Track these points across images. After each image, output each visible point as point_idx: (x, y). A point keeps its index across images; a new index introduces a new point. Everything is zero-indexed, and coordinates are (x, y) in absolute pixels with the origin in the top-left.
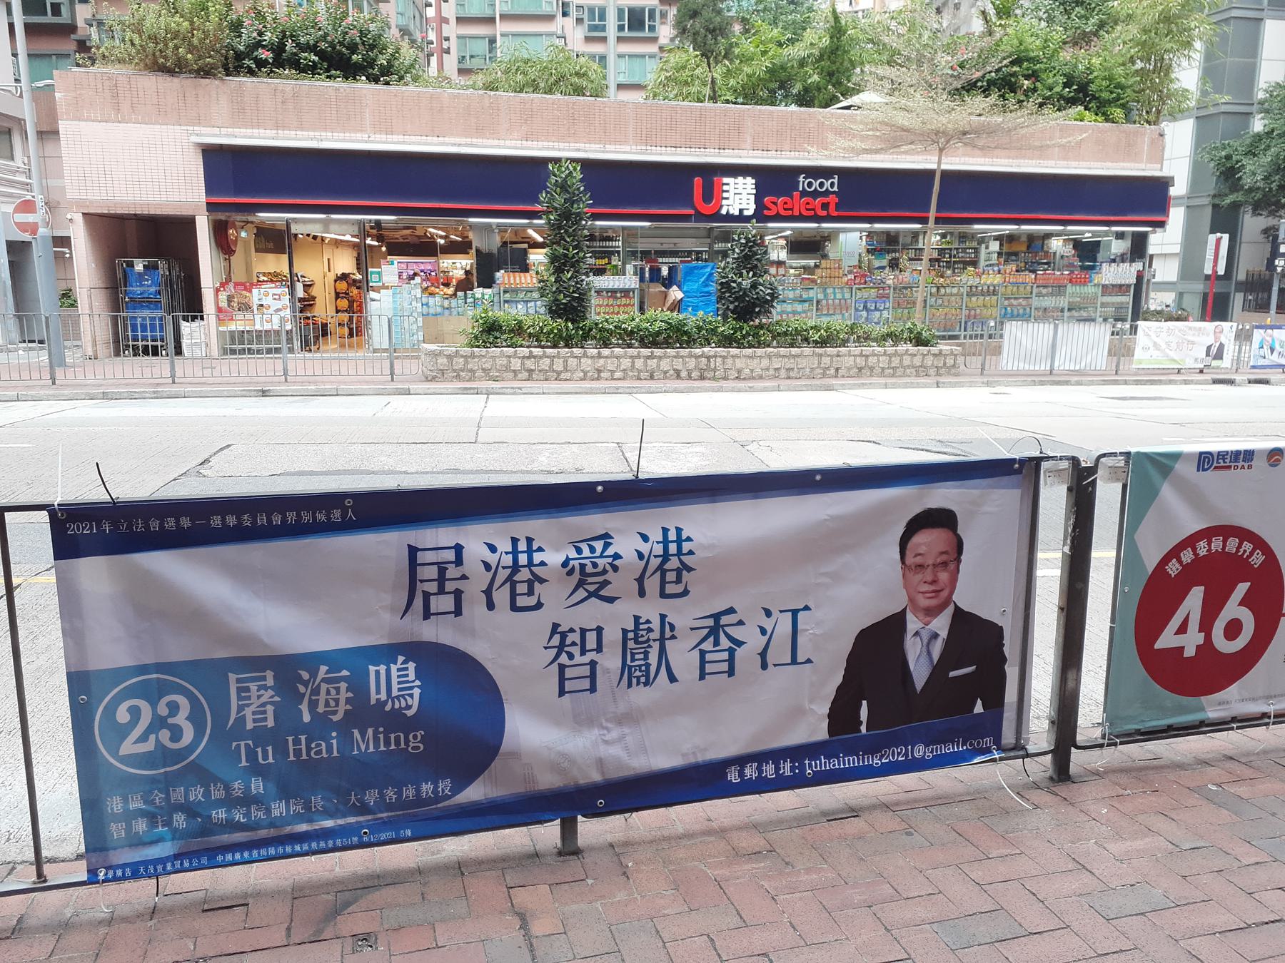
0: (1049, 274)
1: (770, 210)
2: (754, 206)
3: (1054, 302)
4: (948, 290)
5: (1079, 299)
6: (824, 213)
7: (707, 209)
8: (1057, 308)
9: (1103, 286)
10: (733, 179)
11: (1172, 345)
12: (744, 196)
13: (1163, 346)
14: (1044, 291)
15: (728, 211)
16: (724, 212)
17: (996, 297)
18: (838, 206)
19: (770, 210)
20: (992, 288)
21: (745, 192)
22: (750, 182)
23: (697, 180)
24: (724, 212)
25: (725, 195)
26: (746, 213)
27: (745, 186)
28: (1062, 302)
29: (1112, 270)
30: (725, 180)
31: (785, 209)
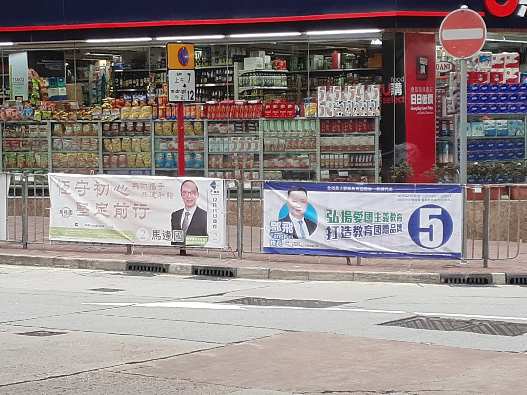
0: (225, 105)
3: (239, 146)
4: (77, 128)
5: (282, 141)
8: (248, 154)
9: (323, 121)
11: (107, 208)
13: (93, 209)
14: (222, 129)
17: (147, 138)
20: (140, 125)
28: (253, 146)
29: (333, 96)
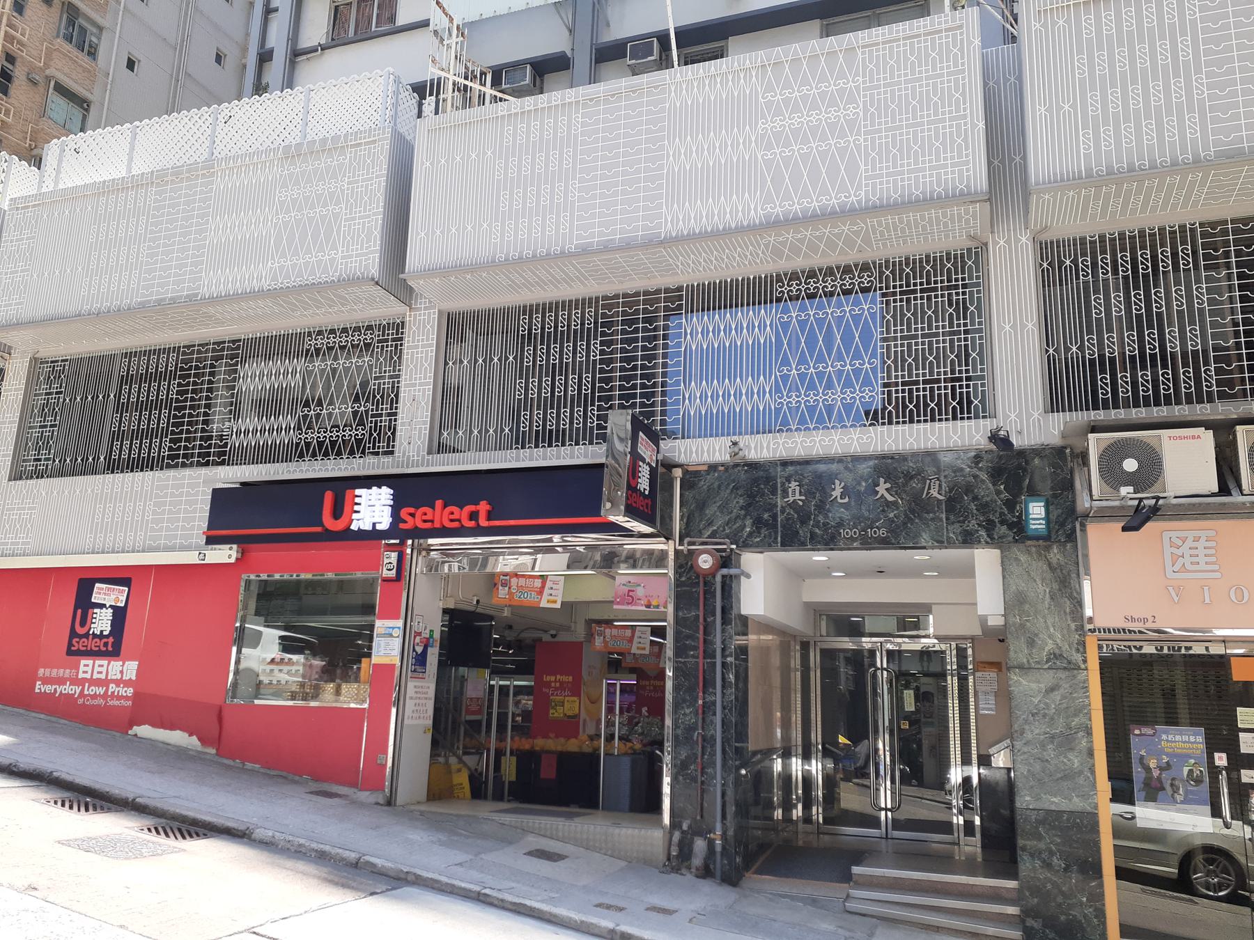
1: (406, 522)
7: (338, 526)
18: (490, 517)
19: (406, 522)
23: (329, 497)
26: (379, 527)
27: (379, 497)
30: (358, 492)
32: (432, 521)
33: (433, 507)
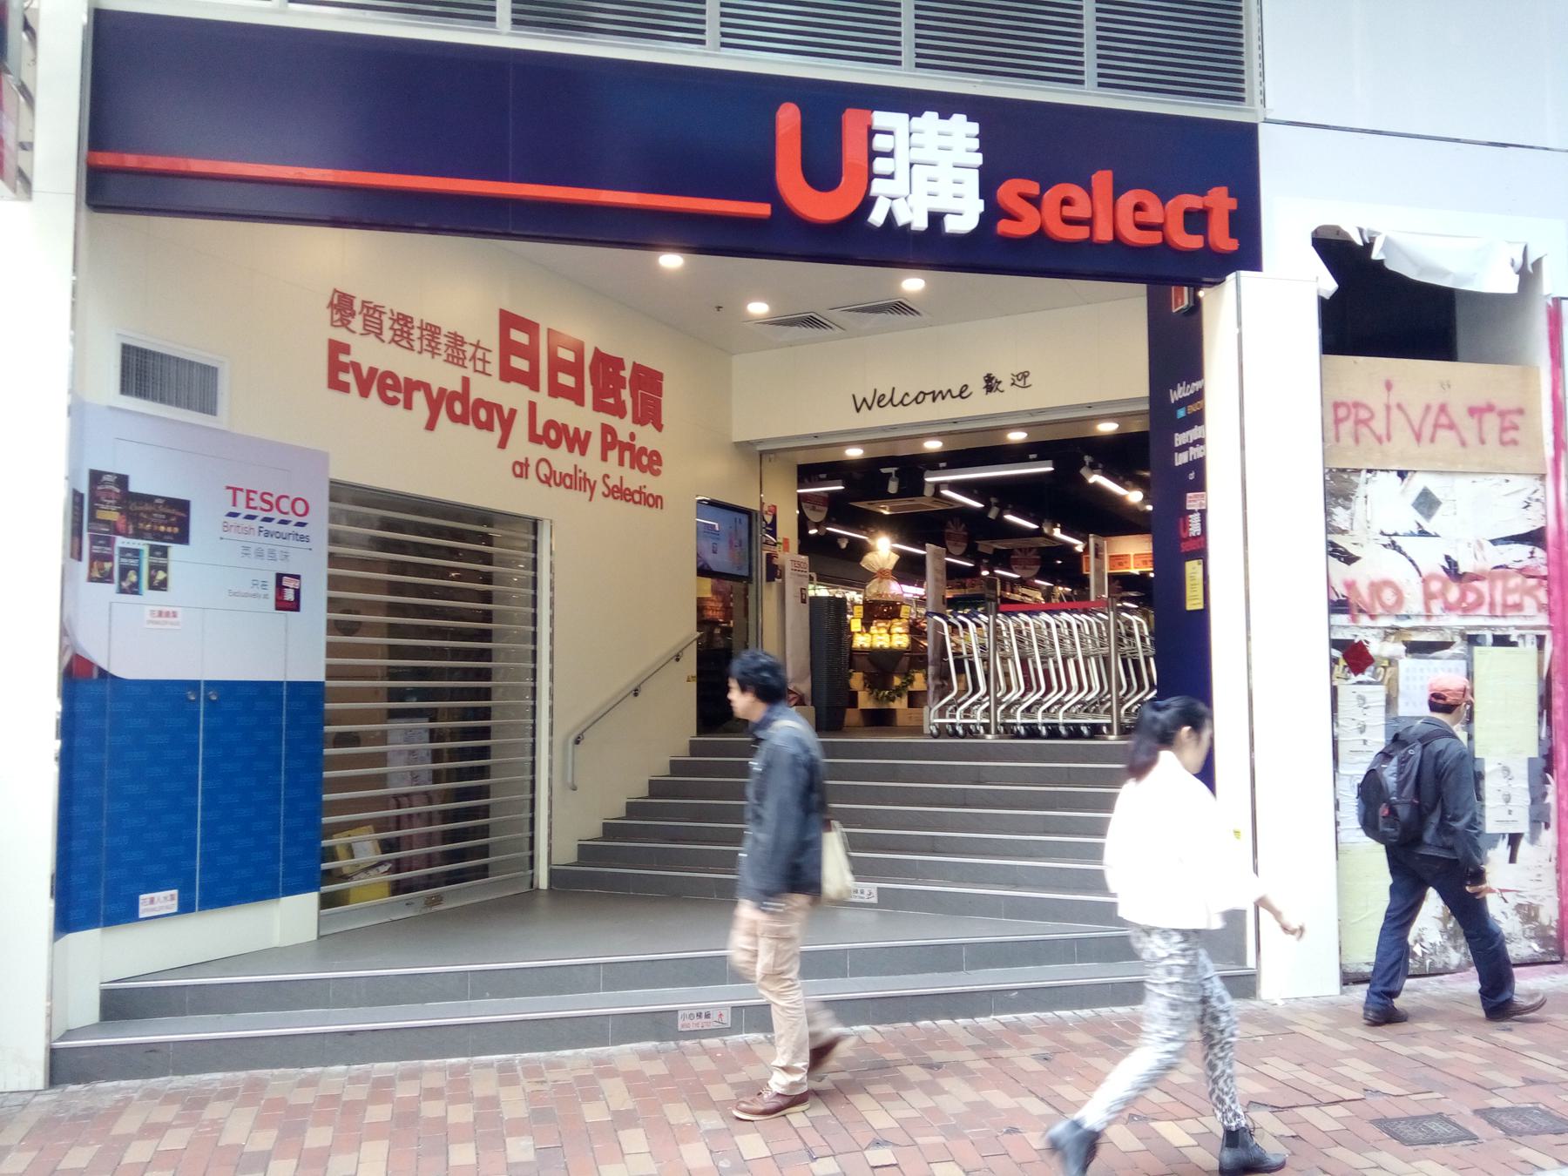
2: (980, 206)
6: (1195, 242)
7: (822, 207)
10: (905, 116)
12: (945, 173)
15: (890, 217)
16: (877, 217)
21: (947, 160)
22: (962, 133)
23: (788, 117)
24: (877, 217)
25: (880, 165)
26: (952, 225)
27: (945, 141)
30: (881, 119)
31: (1069, 221)
32: (1089, 222)
33: (1089, 192)
